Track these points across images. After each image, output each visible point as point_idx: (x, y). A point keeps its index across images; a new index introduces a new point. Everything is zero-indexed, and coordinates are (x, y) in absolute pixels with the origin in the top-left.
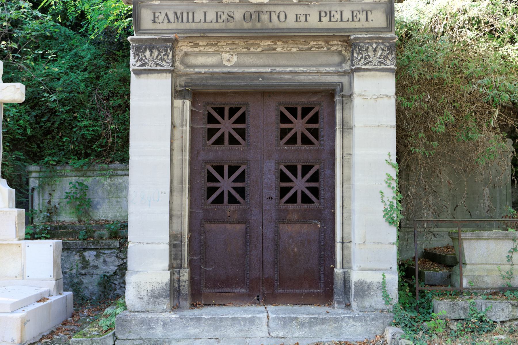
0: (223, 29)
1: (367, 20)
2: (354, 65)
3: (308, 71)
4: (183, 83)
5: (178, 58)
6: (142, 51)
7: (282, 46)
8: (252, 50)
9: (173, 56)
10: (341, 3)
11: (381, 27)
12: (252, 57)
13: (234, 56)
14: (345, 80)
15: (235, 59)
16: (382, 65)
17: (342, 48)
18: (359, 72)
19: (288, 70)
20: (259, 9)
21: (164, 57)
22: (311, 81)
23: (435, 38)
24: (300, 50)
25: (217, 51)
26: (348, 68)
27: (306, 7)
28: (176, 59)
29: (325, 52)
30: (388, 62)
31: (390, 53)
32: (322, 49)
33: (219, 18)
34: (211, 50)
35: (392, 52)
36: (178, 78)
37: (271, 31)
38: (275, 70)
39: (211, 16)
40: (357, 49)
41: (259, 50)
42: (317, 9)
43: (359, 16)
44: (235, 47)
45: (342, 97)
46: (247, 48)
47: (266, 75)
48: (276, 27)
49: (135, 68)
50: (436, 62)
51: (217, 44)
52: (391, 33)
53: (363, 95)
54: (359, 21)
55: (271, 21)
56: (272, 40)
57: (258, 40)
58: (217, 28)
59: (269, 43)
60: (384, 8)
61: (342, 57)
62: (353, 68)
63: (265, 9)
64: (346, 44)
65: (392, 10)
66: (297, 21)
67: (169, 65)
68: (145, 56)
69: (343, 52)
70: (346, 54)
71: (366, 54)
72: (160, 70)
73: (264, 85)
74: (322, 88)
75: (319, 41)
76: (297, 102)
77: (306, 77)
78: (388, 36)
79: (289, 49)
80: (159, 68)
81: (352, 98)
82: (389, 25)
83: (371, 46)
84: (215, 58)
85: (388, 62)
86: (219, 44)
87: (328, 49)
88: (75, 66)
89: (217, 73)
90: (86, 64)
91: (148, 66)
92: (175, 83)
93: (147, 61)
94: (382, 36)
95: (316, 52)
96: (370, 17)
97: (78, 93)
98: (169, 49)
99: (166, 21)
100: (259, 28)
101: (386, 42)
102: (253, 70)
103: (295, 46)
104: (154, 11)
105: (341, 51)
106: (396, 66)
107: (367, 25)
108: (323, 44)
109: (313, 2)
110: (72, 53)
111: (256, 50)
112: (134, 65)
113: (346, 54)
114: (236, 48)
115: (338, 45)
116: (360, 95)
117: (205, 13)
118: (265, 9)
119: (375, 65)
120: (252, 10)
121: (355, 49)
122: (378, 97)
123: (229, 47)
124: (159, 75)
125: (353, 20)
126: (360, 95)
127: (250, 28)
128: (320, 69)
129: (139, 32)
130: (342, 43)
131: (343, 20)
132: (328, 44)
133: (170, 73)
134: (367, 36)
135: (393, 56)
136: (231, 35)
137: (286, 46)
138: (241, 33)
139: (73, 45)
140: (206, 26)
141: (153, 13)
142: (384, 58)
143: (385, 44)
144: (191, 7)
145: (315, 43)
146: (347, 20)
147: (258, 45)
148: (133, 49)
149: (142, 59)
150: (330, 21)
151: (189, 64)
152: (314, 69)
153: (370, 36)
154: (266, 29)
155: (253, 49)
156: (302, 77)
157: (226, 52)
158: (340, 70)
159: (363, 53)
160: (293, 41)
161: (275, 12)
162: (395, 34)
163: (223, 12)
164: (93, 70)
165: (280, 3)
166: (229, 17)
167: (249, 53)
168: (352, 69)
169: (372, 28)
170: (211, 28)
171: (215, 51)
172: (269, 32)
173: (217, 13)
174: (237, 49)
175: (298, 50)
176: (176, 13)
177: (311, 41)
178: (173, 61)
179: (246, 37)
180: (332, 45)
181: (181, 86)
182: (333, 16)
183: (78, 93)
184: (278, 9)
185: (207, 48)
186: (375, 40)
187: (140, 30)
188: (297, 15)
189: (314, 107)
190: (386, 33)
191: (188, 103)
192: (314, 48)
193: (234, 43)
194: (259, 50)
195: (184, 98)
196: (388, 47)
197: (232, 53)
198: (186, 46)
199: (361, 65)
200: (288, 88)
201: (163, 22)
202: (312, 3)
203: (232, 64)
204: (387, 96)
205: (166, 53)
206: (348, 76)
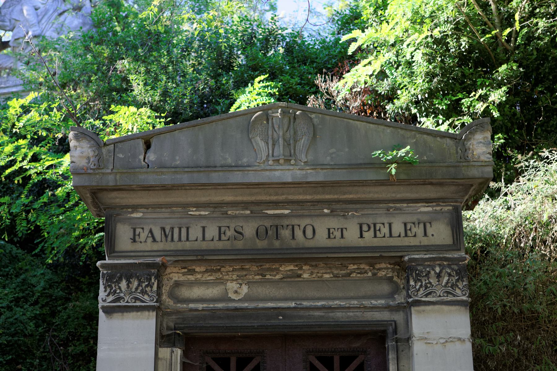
0: (228, 250)
1: (425, 234)
2: (411, 297)
3: (347, 305)
4: (172, 325)
5: (165, 290)
6: (116, 281)
7: (310, 272)
8: (268, 277)
9: (159, 287)
10: (389, 212)
11: (445, 244)
12: (268, 287)
13: (243, 285)
14: (399, 317)
15: (245, 289)
16: (449, 295)
17: (393, 272)
18: (419, 306)
19: (320, 304)
20: (277, 222)
21: (147, 289)
22: (352, 320)
23: (521, 256)
24: (335, 276)
25: (220, 279)
26: (403, 301)
27: (342, 219)
28: (163, 291)
29: (369, 279)
30: (458, 291)
31: (460, 279)
32: (366, 275)
33: (222, 235)
34: (211, 278)
35: (462, 278)
36: (165, 317)
37: (294, 251)
38: (301, 304)
39: (212, 232)
40: (414, 274)
41: (278, 277)
42: (356, 221)
43: (414, 230)
44: (244, 273)
45: (397, 342)
46: (262, 275)
48: (301, 247)
49: (106, 304)
50: (525, 289)
51: (219, 270)
53: (426, 339)
54: (415, 236)
55: (293, 237)
56: (296, 264)
57: (276, 264)
58: (220, 248)
59: (292, 267)
62: (410, 300)
63: (286, 222)
64: (398, 267)
66: (329, 237)
67: (153, 300)
68: (120, 288)
69: (395, 279)
70: (399, 281)
71: (427, 281)
72: (141, 306)
73: (286, 325)
74: (367, 329)
75: (360, 264)
76: (333, 350)
77: (344, 313)
78: (455, 256)
79: (319, 275)
80: (138, 304)
81: (410, 342)
83: (433, 270)
84: (217, 288)
85: (458, 291)
86: (223, 269)
87: (374, 274)
88: (23, 297)
89: (220, 310)
90: (38, 294)
91: (123, 301)
92: (161, 325)
93: (122, 295)
94: (448, 256)
95: (357, 278)
96: (430, 231)
97: (25, 336)
98: (153, 277)
99: (150, 240)
101: (453, 264)
102: (270, 305)
103: (329, 271)
104: (134, 227)
105: (392, 277)
107: (425, 241)
108: (367, 267)
110: (19, 280)
111: (273, 278)
112: (104, 301)
113: (399, 281)
114: (246, 275)
115: (387, 268)
116: (421, 339)
117: (204, 228)
118: (286, 222)
119: (440, 296)
120: (268, 223)
121: (412, 274)
122: (446, 341)
123: (236, 273)
124: (139, 313)
125: (406, 235)
126: (421, 339)
128: (364, 302)
129: (112, 255)
130: (392, 266)
131: (393, 235)
132: (374, 268)
133: (153, 311)
134: (427, 256)
136: (239, 257)
137: (316, 271)
138: (252, 254)
139: (21, 269)
140: (204, 246)
141: (132, 230)
143: (452, 266)
144: (185, 221)
145: (356, 267)
146: (398, 235)
147: (277, 270)
148: (103, 278)
149: (115, 292)
150: (375, 236)
151: (181, 297)
152: (355, 302)
153: (431, 256)
154: (287, 249)
155: (270, 275)
156: (338, 314)
157: (233, 280)
160: (325, 264)
161: (299, 226)
162: (466, 254)
163: (228, 227)
164: (47, 304)
166: (236, 234)
167: (264, 282)
168: (408, 302)
169: (432, 245)
170: (212, 248)
171: (217, 279)
172: (291, 253)
173: (220, 228)
174: (247, 276)
176: (163, 229)
177: (350, 264)
178: (159, 294)
179: (260, 260)
180: (380, 269)
181: (169, 328)
182: (379, 230)
183: (25, 336)
184: (304, 222)
185: (206, 275)
186: (438, 262)
187: (114, 252)
188: (329, 230)
189: (358, 356)
191: (178, 352)
192: (355, 274)
193: (243, 269)
194: (278, 277)
195: (173, 345)
197: (241, 282)
198: (178, 273)
199: (420, 296)
200: (319, 329)
201: (145, 242)
202: (350, 214)
203: (240, 297)
204: (459, 339)
205: (149, 284)
206: (403, 311)
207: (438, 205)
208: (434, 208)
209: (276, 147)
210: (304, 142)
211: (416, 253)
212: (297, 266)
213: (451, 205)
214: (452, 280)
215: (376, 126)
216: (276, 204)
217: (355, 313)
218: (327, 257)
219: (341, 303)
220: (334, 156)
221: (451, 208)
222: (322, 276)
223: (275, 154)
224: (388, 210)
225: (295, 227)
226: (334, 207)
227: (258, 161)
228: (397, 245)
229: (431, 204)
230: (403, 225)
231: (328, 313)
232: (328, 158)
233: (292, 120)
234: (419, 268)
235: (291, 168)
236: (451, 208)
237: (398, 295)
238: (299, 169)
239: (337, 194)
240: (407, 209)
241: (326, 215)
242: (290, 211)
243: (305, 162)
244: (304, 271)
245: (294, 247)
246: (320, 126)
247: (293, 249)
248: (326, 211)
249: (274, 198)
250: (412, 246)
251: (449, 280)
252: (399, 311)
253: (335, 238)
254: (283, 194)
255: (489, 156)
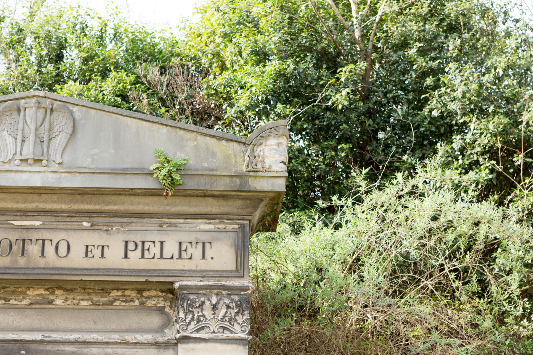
7: (64, 297)
8: (12, 302)
10: (162, 229)
16: (226, 332)
17: (166, 301)
18: (187, 343)
19: (72, 337)
20: (25, 235)
24: (94, 304)
27: (103, 234)
30: (237, 327)
32: (132, 304)
35: (243, 311)
37: (43, 272)
38: (49, 337)
40: (185, 304)
41: (25, 302)
43: (190, 251)
47: (33, 346)
48: (51, 266)
52: (242, 279)
55: (43, 255)
57: (23, 286)
60: (232, 239)
61: (166, 317)
62: (178, 336)
64: (172, 296)
65: (244, 242)
66: (87, 256)
69: (167, 309)
70: (171, 312)
71: (200, 314)
75: (126, 289)
77: (101, 350)
82: (239, 267)
85: (237, 327)
87: (142, 304)
96: (209, 253)
100: (23, 266)
101: (234, 294)
103: (87, 297)
105: (164, 307)
106: (250, 333)
107: (203, 265)
108: (133, 294)
109: (116, 226)
111: (19, 303)
113: (171, 312)
118: (34, 235)
119: (214, 332)
120: (13, 236)
121: (182, 305)
125: (180, 257)
127: (7, 266)
128: (126, 337)
130: (164, 294)
131: (164, 256)
132: (142, 296)
134: (202, 283)
135: (245, 318)
137: (71, 297)
142: (230, 321)
143: (233, 297)
145: (120, 293)
152: (116, 337)
153: (207, 283)
154: (34, 269)
155: (15, 300)
158: (160, 340)
159: (195, 311)
161: (51, 240)
165: (60, 227)
169: (211, 271)
175: (91, 303)
177: (113, 290)
182: (148, 250)
184: (56, 236)
186: (215, 291)
188: (87, 246)
190: (234, 279)
192: (119, 302)
194: (25, 302)
196: (236, 303)
206: (173, 349)
207: (221, 223)
208: (217, 226)
209: (26, 144)
210: (60, 140)
211: (190, 278)
212: (47, 289)
213: (237, 224)
214: (230, 313)
215: (150, 124)
216: (24, 213)
217: (115, 350)
218: (81, 280)
219: (99, 337)
220: (95, 157)
221: (236, 226)
222: (78, 304)
223: (23, 153)
224: (162, 227)
225: (46, 242)
226: (96, 220)
227: (1, 160)
228: (167, 268)
229: (213, 221)
230: (178, 244)
231: (82, 348)
232: (89, 160)
233: (48, 112)
234: (192, 297)
235: (42, 169)
236: (236, 226)
237: (169, 329)
238: (52, 172)
239: (98, 204)
240: (184, 225)
241: (86, 229)
242: (41, 223)
243: (59, 164)
244: (57, 297)
245: (43, 266)
246: (83, 122)
247: (40, 269)
248: (85, 224)
249: (22, 206)
250: (186, 271)
251: (226, 312)
252: (169, 349)
253: (93, 257)
254: (33, 202)
255: (282, 165)
